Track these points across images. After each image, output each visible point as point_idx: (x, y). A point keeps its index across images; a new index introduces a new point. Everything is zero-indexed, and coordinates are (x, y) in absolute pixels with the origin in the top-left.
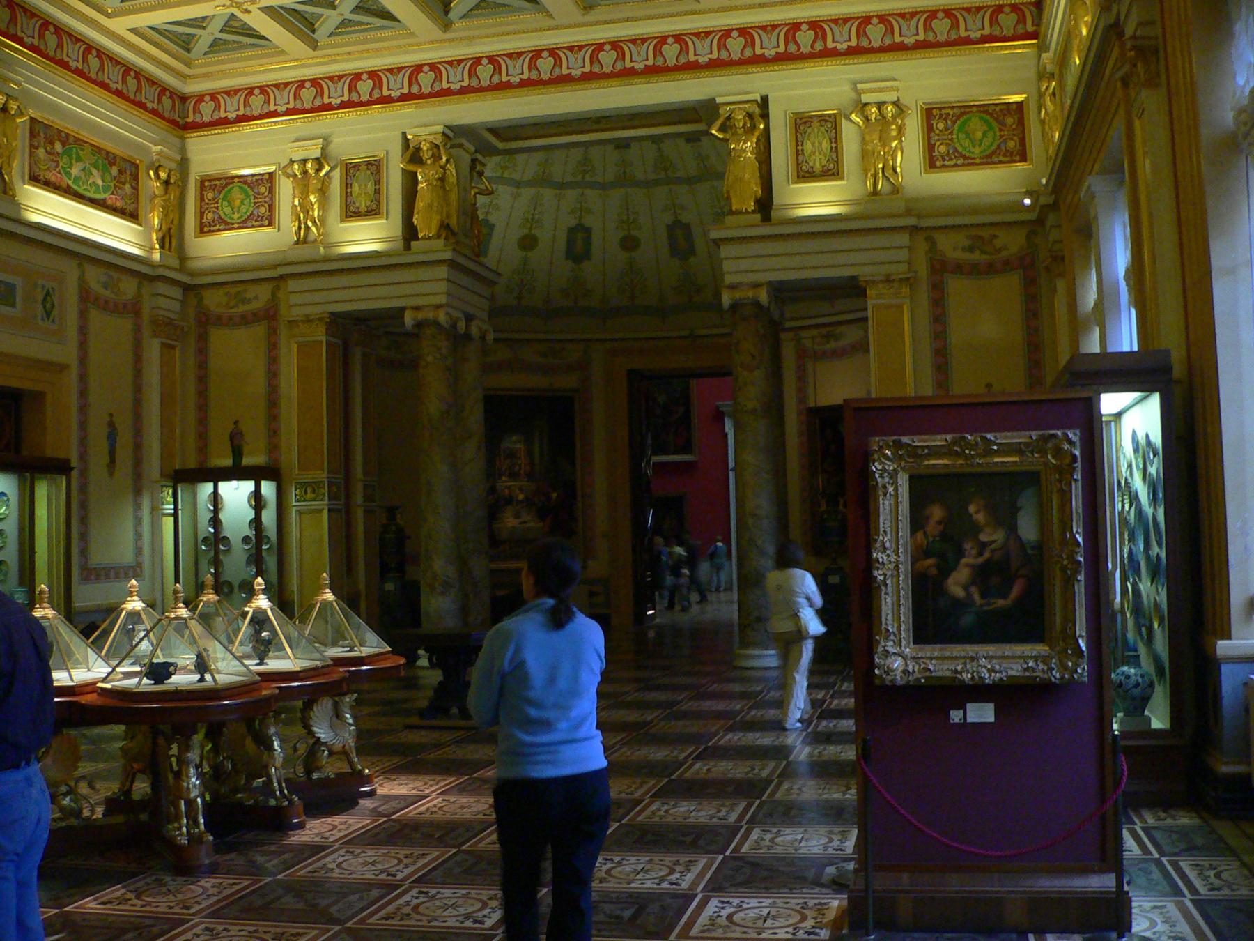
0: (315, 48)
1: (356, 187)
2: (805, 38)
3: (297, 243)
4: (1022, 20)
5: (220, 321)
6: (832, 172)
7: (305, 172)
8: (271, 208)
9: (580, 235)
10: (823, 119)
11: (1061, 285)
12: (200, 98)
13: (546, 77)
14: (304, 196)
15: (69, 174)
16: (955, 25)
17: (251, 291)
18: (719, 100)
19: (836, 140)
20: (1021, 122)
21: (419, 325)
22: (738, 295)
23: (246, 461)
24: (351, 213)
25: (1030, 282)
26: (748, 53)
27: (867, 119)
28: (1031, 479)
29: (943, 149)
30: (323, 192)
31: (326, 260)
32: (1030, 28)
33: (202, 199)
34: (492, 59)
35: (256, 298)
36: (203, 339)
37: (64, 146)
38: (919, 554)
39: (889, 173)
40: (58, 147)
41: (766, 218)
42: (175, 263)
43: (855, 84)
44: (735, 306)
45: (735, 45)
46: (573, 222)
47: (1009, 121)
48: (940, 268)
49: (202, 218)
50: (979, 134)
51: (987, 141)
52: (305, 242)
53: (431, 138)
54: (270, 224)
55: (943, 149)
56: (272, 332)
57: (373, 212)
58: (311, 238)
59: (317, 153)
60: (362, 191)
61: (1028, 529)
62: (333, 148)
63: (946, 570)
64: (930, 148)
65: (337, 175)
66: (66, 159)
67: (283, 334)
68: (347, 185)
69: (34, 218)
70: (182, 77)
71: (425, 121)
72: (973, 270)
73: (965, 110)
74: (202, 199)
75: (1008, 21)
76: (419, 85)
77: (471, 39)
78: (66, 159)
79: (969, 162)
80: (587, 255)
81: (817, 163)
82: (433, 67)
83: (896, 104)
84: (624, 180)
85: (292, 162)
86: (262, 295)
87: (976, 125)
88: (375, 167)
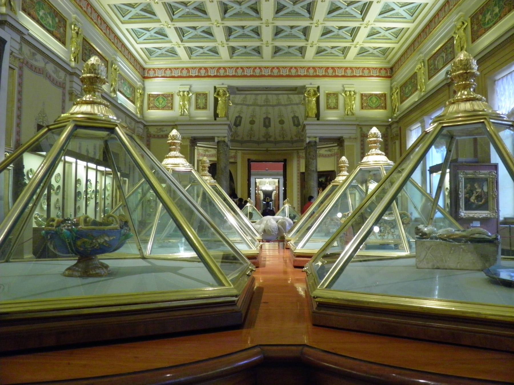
0: (190, 59)
1: (199, 101)
2: (330, 71)
3: (181, 115)
4: (387, 72)
5: (154, 137)
6: (336, 108)
7: (184, 95)
8: (172, 104)
9: (239, 119)
10: (334, 94)
11: (397, 143)
12: (150, 69)
13: (258, 75)
14: (184, 101)
16: (370, 72)
18: (307, 86)
19: (337, 100)
20: (385, 99)
24: (198, 108)
26: (315, 74)
27: (346, 95)
28: (486, 180)
29: (365, 104)
30: (189, 100)
32: (389, 75)
33: (149, 100)
34: (242, 68)
38: (466, 193)
39: (351, 109)
41: (318, 119)
42: (142, 118)
44: (309, 142)
45: (311, 72)
46: (265, 116)
47: (382, 98)
49: (149, 104)
50: (375, 101)
51: (377, 103)
52: (183, 115)
53: (224, 89)
54: (172, 109)
55: (365, 104)
57: (205, 108)
58: (185, 114)
59: (188, 90)
60: (201, 102)
61: (485, 189)
62: (192, 89)
63: (470, 197)
64: (362, 104)
65: (194, 97)
68: (197, 100)
69: (119, 102)
70: (145, 62)
71: (222, 83)
73: (371, 95)
74: (149, 100)
75: (383, 73)
76: (219, 73)
77: (237, 62)
79: (372, 108)
80: (239, 125)
81: (332, 105)
83: (354, 91)
84: (255, 104)
85: (180, 92)
87: (374, 99)
88: (205, 95)
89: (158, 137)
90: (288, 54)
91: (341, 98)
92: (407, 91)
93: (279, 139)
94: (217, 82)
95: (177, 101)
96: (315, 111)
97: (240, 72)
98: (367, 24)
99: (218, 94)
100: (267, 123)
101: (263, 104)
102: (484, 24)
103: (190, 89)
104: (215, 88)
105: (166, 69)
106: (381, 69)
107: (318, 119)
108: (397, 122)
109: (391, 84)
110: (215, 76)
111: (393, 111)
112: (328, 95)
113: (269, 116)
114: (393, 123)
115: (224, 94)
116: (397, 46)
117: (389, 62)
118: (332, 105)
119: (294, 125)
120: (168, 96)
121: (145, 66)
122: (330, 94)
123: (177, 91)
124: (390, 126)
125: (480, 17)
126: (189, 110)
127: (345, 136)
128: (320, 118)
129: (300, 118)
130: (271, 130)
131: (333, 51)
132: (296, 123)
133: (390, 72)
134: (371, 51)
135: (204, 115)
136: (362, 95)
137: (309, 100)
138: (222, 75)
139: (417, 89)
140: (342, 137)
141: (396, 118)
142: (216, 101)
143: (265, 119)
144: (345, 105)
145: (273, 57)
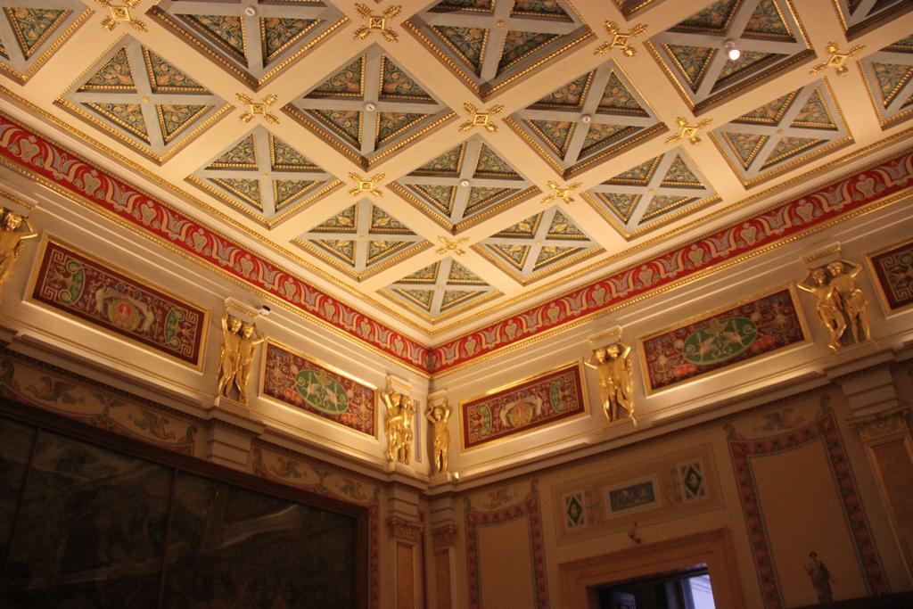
15: (305, 393)
35: (516, 495)
36: (472, 536)
37: (299, 369)
40: (294, 369)
66: (301, 380)
78: (301, 380)
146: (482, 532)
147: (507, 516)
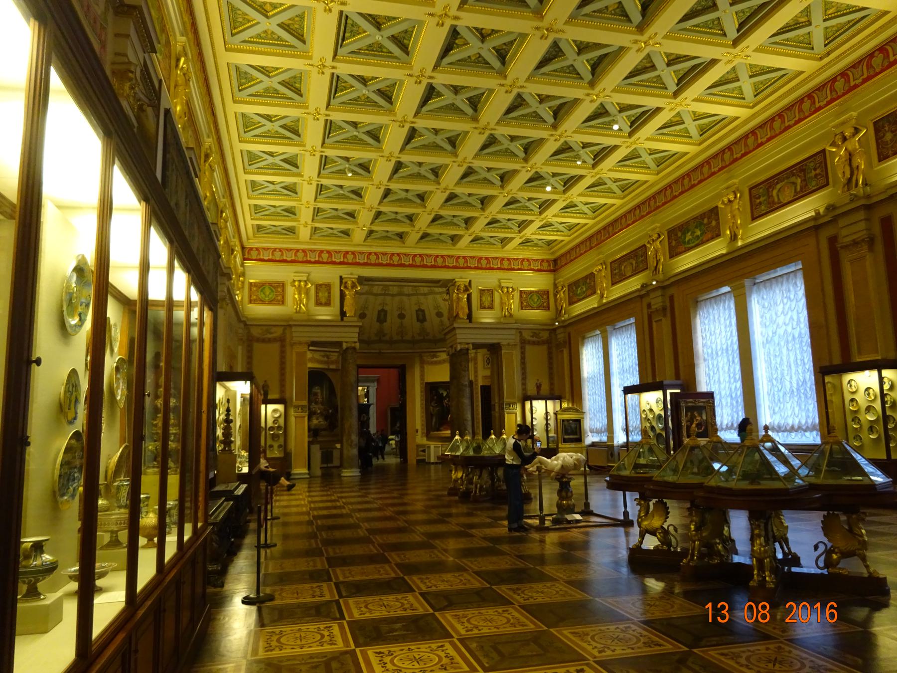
1: (320, 294)
2: (484, 262)
4: (549, 265)
5: (259, 340)
6: (491, 307)
7: (299, 286)
10: (488, 290)
12: (251, 249)
14: (300, 294)
17: (273, 330)
20: (548, 298)
21: (347, 348)
22: (463, 346)
23: (270, 397)
24: (318, 303)
25: (549, 348)
30: (307, 292)
31: (309, 320)
41: (470, 321)
43: (499, 280)
44: (461, 350)
48: (523, 342)
49: (251, 296)
56: (283, 346)
57: (328, 304)
60: (323, 296)
62: (312, 277)
64: (522, 303)
67: (288, 348)
68: (317, 293)
71: (351, 273)
72: (534, 343)
75: (545, 265)
77: (371, 246)
79: (533, 308)
81: (487, 304)
82: (353, 253)
86: (278, 332)
87: (535, 298)
88: (328, 286)
89: (264, 341)
90: (438, 240)
91: (497, 296)
92: (579, 291)
93: (395, 338)
94: (344, 271)
95: (291, 293)
96: (467, 311)
97: (373, 258)
98: (543, 219)
99: (345, 287)
100: (382, 316)
101: (379, 292)
102: (684, 243)
103: (308, 277)
104: (341, 278)
105: (275, 250)
106: (543, 261)
107: (470, 321)
108: (564, 327)
109: (555, 280)
110: (341, 263)
111: (559, 312)
112: (482, 292)
113: (386, 308)
114: (559, 327)
115: (354, 286)
116: (567, 239)
117: (553, 253)
118: (487, 304)
119: (418, 320)
120: (278, 287)
121: (246, 245)
122: (484, 290)
123: (290, 280)
124: (555, 330)
125: (679, 234)
126: (306, 306)
127: (504, 342)
128: (473, 320)
129: (427, 313)
130: (386, 325)
131: (492, 240)
132: (421, 317)
133: (554, 266)
134: (536, 241)
135: (325, 314)
136: (521, 291)
137: (458, 298)
138: (350, 261)
139: (594, 293)
140: (499, 344)
141: (564, 321)
142: (342, 295)
143: (379, 311)
144: (502, 304)
145: (417, 243)
146: (257, 346)
147: (270, 341)
